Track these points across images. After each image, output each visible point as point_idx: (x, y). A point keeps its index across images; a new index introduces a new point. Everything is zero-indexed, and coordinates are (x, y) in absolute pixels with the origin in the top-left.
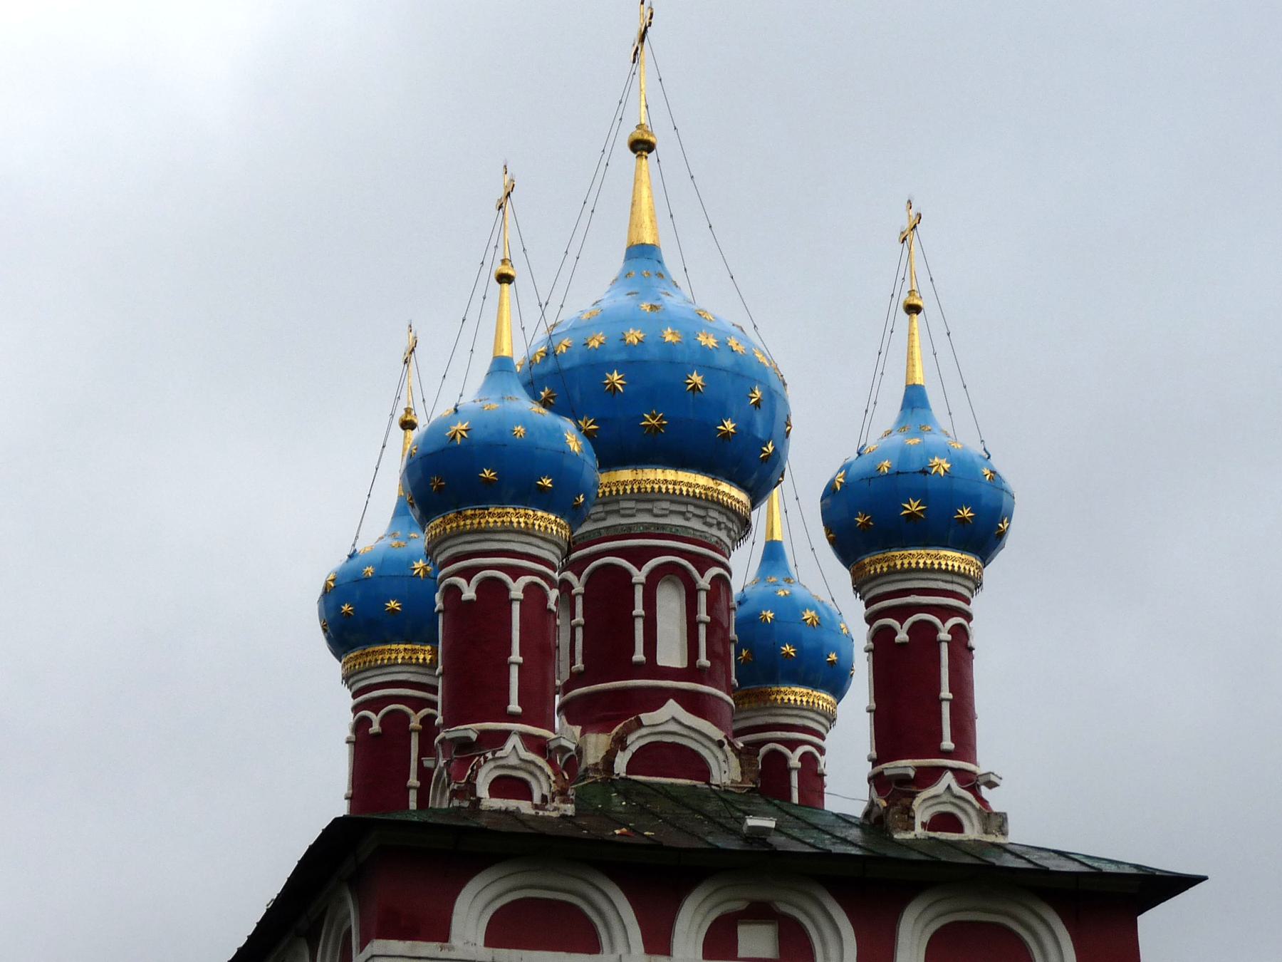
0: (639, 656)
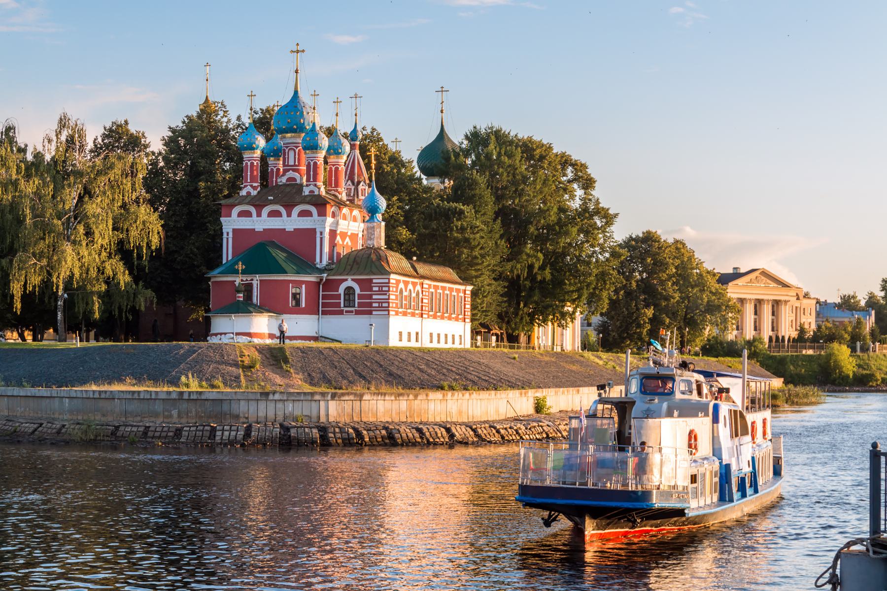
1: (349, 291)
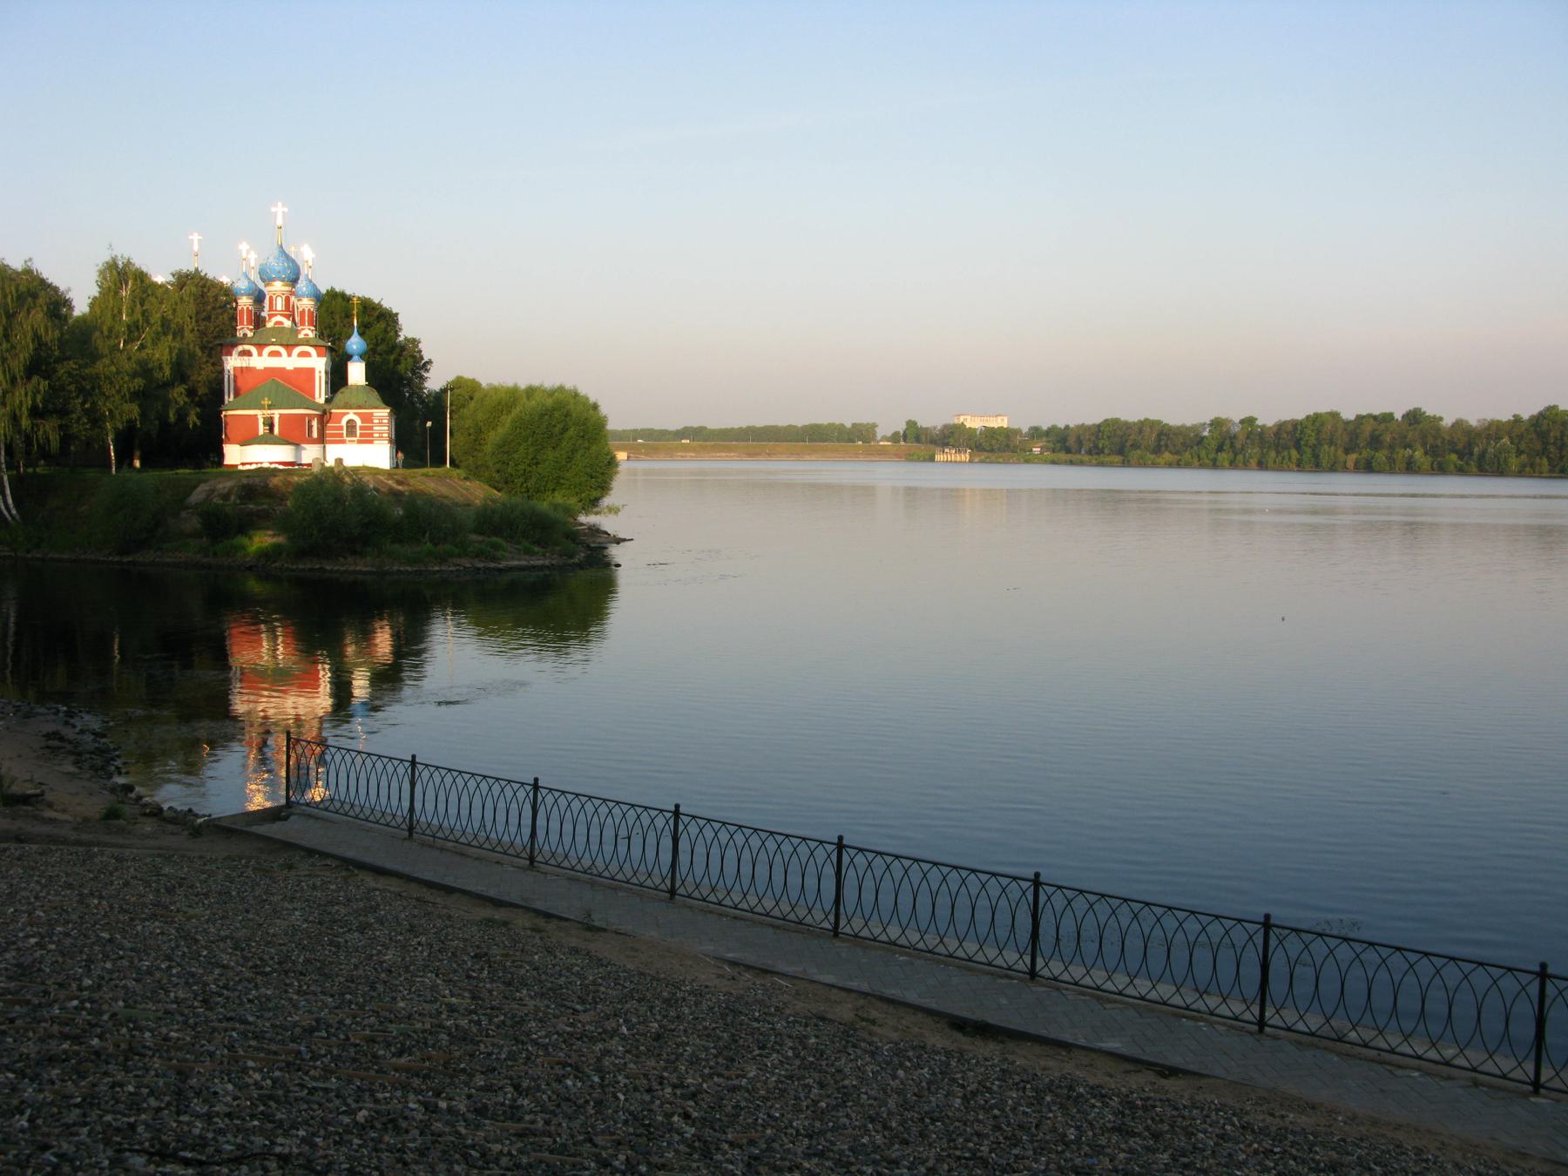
1: (351, 425)
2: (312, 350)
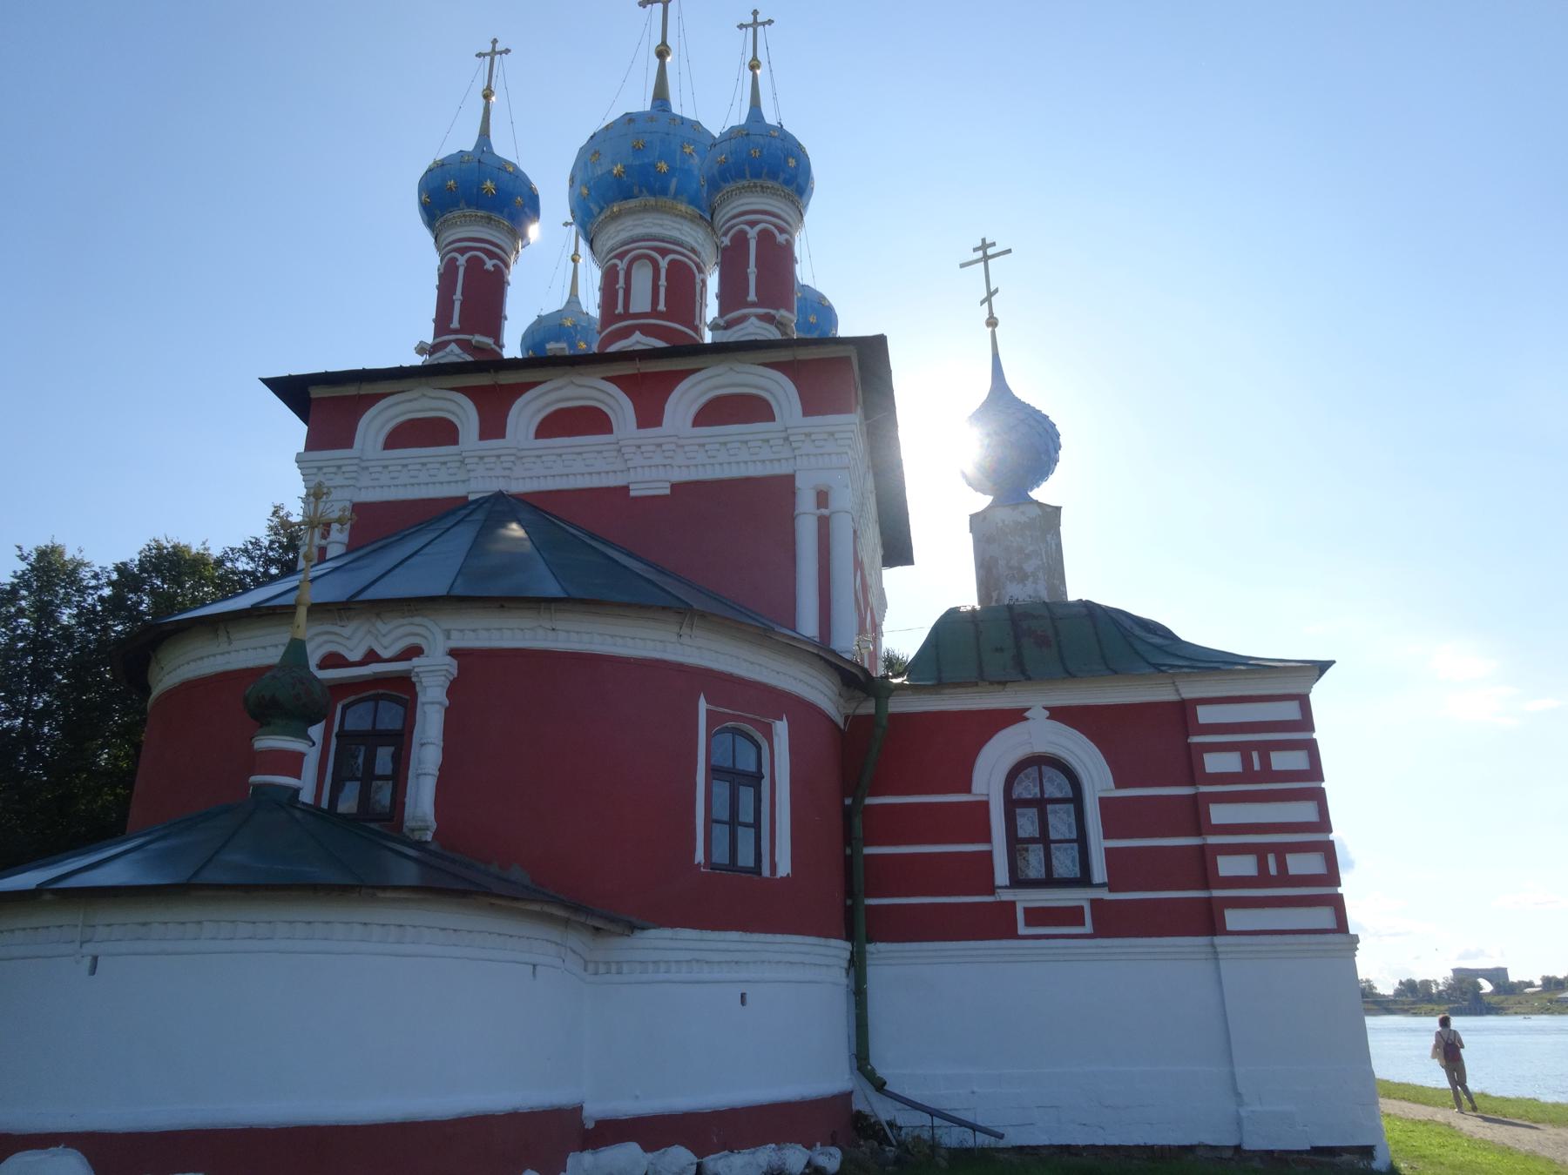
0: (620, 309)
2: (780, 390)
